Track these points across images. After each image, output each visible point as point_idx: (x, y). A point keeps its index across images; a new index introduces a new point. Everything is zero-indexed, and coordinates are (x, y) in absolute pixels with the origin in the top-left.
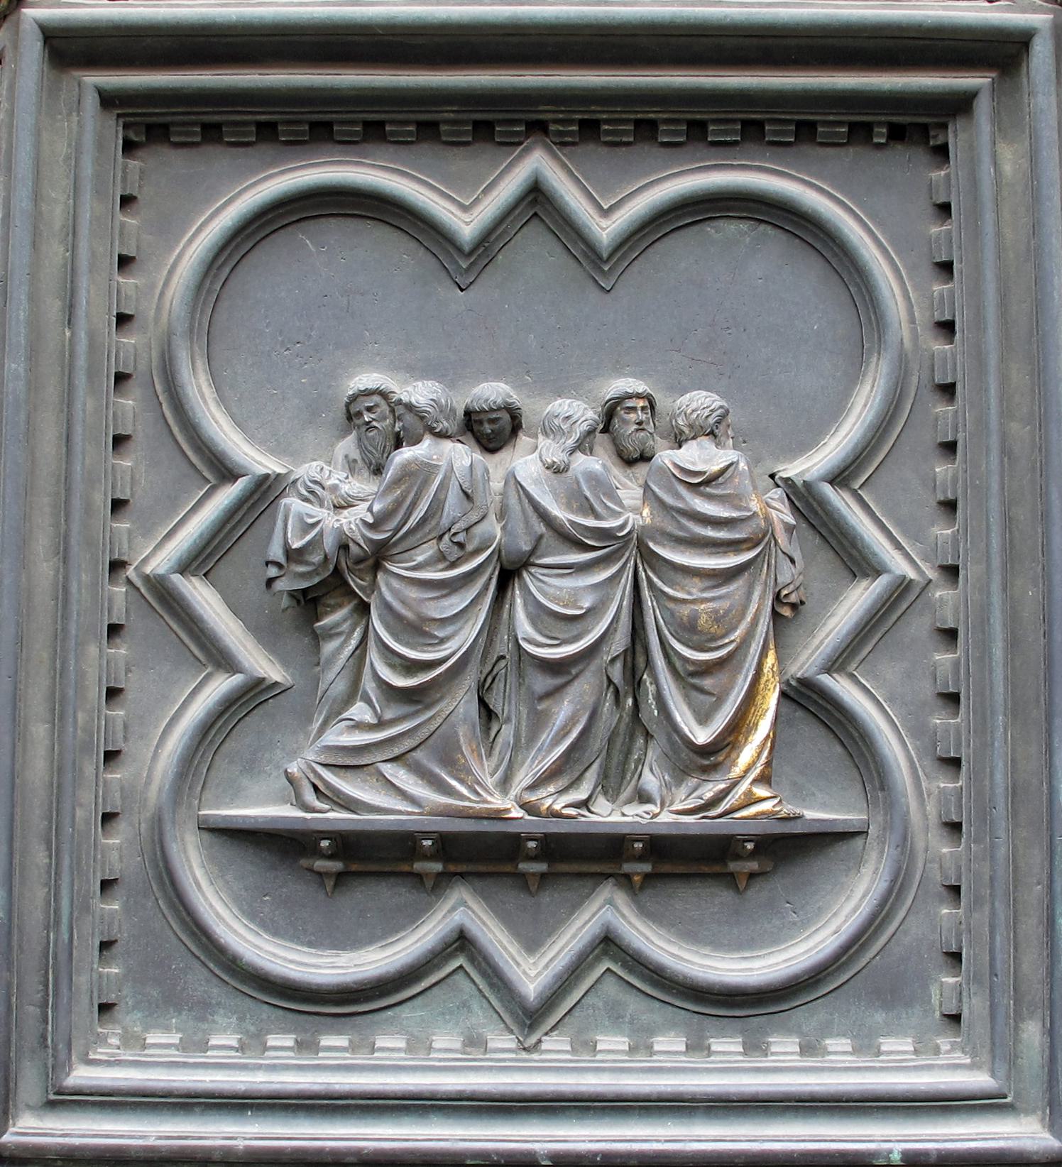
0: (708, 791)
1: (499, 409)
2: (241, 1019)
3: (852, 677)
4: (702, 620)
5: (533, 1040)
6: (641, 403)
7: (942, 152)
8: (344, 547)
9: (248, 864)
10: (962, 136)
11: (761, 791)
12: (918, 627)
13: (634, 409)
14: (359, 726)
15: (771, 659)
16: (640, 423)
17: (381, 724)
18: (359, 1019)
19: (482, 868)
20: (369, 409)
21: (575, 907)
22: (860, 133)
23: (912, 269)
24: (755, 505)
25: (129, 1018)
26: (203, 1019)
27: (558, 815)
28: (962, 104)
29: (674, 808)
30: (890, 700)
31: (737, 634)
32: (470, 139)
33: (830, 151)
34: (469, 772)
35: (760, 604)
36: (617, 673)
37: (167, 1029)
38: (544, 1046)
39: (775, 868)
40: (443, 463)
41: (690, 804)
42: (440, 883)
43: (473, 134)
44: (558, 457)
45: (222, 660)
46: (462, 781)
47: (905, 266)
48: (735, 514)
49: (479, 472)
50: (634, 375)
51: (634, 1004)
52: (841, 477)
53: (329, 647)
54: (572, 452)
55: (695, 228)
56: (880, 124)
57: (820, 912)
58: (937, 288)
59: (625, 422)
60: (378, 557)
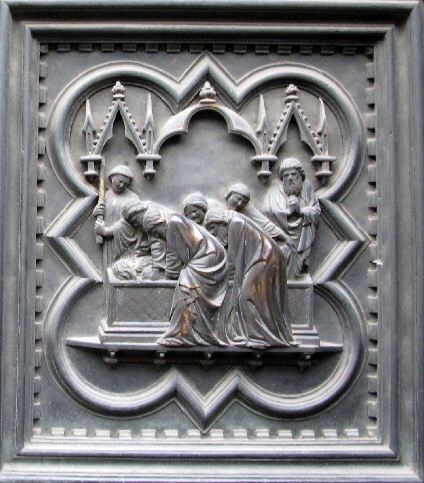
32: (92, 50)
43: (70, 48)
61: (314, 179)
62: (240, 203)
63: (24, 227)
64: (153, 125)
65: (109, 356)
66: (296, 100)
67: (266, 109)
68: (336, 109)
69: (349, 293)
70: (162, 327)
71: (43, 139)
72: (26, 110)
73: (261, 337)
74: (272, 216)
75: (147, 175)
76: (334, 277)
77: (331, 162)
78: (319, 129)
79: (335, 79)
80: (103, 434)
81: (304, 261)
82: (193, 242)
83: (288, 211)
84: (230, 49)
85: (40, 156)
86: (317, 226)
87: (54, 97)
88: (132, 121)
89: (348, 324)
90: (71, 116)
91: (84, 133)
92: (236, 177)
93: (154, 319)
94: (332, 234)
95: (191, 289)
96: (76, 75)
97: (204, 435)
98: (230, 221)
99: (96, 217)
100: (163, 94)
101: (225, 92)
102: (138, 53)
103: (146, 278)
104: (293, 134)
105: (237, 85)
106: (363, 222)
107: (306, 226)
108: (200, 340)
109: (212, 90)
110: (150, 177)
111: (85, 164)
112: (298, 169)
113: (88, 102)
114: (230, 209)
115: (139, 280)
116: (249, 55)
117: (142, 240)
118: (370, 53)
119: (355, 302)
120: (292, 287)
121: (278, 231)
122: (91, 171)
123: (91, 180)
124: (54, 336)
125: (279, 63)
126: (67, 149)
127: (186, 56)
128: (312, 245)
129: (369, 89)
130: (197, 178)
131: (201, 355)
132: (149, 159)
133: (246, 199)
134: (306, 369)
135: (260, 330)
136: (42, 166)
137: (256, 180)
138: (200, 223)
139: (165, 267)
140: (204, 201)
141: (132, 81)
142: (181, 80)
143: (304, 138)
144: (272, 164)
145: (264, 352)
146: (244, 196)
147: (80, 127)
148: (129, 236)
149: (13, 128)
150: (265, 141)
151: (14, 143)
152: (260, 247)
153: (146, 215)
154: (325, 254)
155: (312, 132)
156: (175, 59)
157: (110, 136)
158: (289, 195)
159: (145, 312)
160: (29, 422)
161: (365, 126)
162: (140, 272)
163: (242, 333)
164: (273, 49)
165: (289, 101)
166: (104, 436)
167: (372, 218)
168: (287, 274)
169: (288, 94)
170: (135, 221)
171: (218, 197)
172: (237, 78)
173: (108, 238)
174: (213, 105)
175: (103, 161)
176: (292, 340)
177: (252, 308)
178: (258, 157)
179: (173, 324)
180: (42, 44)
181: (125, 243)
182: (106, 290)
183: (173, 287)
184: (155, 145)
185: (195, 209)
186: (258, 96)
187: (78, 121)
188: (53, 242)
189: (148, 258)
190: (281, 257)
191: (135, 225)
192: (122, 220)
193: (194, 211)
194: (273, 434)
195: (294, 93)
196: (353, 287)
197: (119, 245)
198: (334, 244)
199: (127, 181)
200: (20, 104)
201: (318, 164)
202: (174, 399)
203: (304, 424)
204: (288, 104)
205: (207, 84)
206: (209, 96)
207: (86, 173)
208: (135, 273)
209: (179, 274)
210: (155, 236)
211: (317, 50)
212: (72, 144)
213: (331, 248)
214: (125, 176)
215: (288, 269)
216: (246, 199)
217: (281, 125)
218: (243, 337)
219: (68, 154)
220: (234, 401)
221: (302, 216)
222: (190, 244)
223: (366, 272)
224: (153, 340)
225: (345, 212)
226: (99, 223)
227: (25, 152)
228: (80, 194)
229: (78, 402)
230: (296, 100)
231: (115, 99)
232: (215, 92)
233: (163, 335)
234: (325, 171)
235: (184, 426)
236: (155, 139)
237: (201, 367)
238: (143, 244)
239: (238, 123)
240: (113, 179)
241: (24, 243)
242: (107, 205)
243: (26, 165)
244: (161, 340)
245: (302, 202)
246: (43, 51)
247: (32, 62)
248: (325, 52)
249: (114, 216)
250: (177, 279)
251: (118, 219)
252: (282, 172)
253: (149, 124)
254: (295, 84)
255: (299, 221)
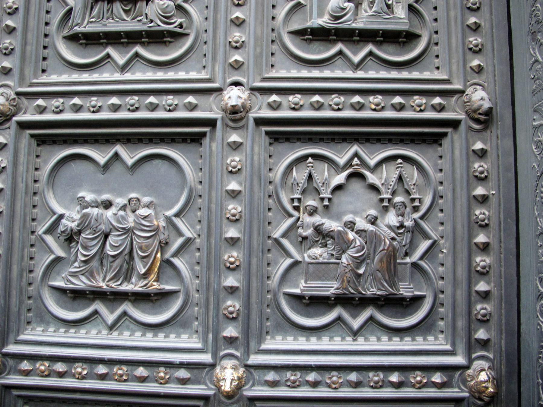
0: (144, 283)
1: (106, 201)
2: (55, 326)
3: (178, 258)
4: (143, 247)
5: (111, 332)
6: (135, 200)
7: (201, 144)
8: (72, 230)
9: (57, 293)
10: (205, 141)
11: (155, 283)
12: (193, 247)
13: (133, 201)
14: (76, 267)
15: (159, 255)
16: (135, 204)
17: (80, 267)
18: (78, 327)
19: (102, 297)
20: (81, 201)
21: (120, 305)
22: (184, 141)
23: (195, 170)
24: (155, 222)
25: (34, 325)
26: (48, 325)
27: (113, 287)
28: (204, 134)
29: (139, 286)
30: (187, 263)
31: (150, 250)
33: (179, 144)
34: (95, 278)
35: (156, 243)
36: (127, 257)
37: (41, 327)
38: (113, 334)
39: (161, 298)
40: (92, 213)
41: (142, 285)
42: (93, 300)
44: (115, 212)
45: (52, 252)
46: (94, 280)
47: (194, 169)
48: (150, 224)
49: (99, 215)
50: (136, 193)
51: (132, 326)
52: (177, 215)
53: (72, 250)
54: (118, 210)
55: (150, 161)
56: (189, 139)
57: (170, 308)
58: (200, 174)
59: (132, 204)
60: (79, 232)
61: (411, 208)
62: (373, 220)
63: (261, 233)
64: (328, 180)
65: (305, 299)
66: (402, 167)
67: (386, 172)
68: (423, 172)
69: (429, 267)
70: (333, 284)
71: (271, 187)
72: (262, 172)
73: (384, 289)
74: (390, 227)
75: (325, 206)
76: (421, 258)
77: (420, 199)
78: (414, 182)
79: (422, 156)
80: (302, 339)
81: (406, 250)
82: (349, 240)
83: (398, 225)
84: (368, 140)
85: (270, 196)
86: (413, 232)
87: (277, 166)
88: (317, 178)
89: (429, 283)
90: (286, 175)
91: (292, 184)
92: (371, 207)
93: (329, 280)
94: (420, 236)
95: (347, 265)
96: (288, 154)
97: (354, 340)
98: (368, 229)
99: (298, 227)
100: (333, 164)
101: (366, 163)
102: (320, 143)
103: (324, 259)
104: (400, 185)
105: (371, 159)
106: (436, 230)
107: (407, 232)
108: (352, 291)
109: (358, 162)
110: (326, 207)
111: (293, 200)
112: (403, 202)
113: (294, 168)
114: (368, 223)
115: (321, 260)
116: (377, 144)
117: (322, 239)
118: (440, 143)
119: (433, 271)
120: (400, 264)
121: (393, 235)
122: (296, 204)
123: (296, 208)
124: (277, 289)
125: (393, 148)
126: (283, 192)
127: (345, 144)
128: (410, 242)
129: (440, 162)
130: (351, 207)
131: (353, 299)
132: (326, 198)
133: (376, 218)
134: (407, 306)
135: (383, 286)
136: (270, 201)
137: (381, 208)
138: (352, 231)
139: (334, 253)
140: (354, 219)
141: (317, 157)
142: (343, 157)
143: (406, 187)
144: (389, 200)
145: (385, 297)
146: (375, 217)
147: (290, 181)
148: (316, 237)
149: (255, 182)
150: (386, 188)
151: (256, 189)
152: (383, 243)
153: (324, 226)
154: (417, 247)
155: (410, 183)
156: (339, 146)
157: (306, 186)
158: (398, 216)
159: (324, 276)
160: (264, 333)
161: (438, 180)
162: (321, 256)
163: (374, 287)
164: (390, 141)
165: (398, 168)
166: (303, 341)
167: (441, 228)
168: (397, 257)
169: (398, 164)
170: (319, 230)
171: (361, 217)
172: (372, 156)
173: (305, 238)
174: (359, 170)
175: (302, 198)
176: (400, 291)
177: (379, 275)
178: (382, 196)
179: (338, 283)
180: (270, 138)
181: (314, 241)
182: (304, 265)
183: (338, 264)
184: (329, 190)
185: (349, 223)
186: (382, 165)
187: (289, 178)
188: (276, 240)
189: (325, 249)
190: (394, 248)
191: (319, 231)
192: (312, 229)
193: (349, 225)
194: (390, 339)
195: (401, 163)
196: (431, 264)
197: (310, 242)
198: (421, 241)
199: (314, 209)
200: (259, 169)
201: (413, 200)
202: (339, 321)
203: (406, 334)
204: (398, 169)
205: (356, 159)
206: (357, 165)
207: (293, 205)
208: (319, 257)
209: (341, 257)
210: (329, 237)
211: (413, 141)
212: (286, 190)
213: (420, 243)
214: (313, 206)
215: (398, 254)
216: (376, 218)
217: (394, 180)
218: (375, 290)
219: (284, 195)
220: (369, 322)
221: (405, 227)
222: (347, 242)
223: (438, 256)
224: (328, 291)
225: (427, 225)
226: (300, 230)
227: (262, 194)
228: (290, 216)
229: (289, 323)
230: (402, 167)
231: (308, 167)
232: (360, 163)
233: (333, 289)
234: (417, 203)
235: (344, 335)
236: (329, 187)
237: (353, 305)
238: (323, 241)
239: (372, 179)
240: (307, 208)
241: (261, 241)
242: (304, 221)
243: (262, 201)
244: (332, 291)
245: (405, 220)
246: (271, 142)
247: (265, 147)
248: (417, 142)
249: (308, 227)
250: (340, 259)
251: (310, 228)
252: (395, 204)
253: (326, 179)
254: (401, 159)
255: (403, 229)
